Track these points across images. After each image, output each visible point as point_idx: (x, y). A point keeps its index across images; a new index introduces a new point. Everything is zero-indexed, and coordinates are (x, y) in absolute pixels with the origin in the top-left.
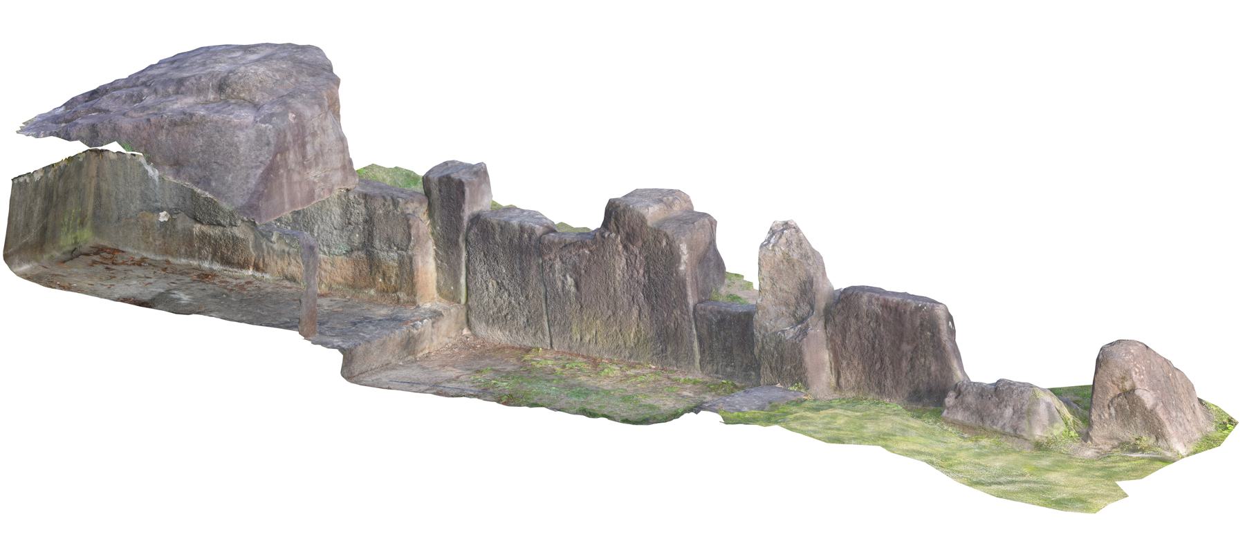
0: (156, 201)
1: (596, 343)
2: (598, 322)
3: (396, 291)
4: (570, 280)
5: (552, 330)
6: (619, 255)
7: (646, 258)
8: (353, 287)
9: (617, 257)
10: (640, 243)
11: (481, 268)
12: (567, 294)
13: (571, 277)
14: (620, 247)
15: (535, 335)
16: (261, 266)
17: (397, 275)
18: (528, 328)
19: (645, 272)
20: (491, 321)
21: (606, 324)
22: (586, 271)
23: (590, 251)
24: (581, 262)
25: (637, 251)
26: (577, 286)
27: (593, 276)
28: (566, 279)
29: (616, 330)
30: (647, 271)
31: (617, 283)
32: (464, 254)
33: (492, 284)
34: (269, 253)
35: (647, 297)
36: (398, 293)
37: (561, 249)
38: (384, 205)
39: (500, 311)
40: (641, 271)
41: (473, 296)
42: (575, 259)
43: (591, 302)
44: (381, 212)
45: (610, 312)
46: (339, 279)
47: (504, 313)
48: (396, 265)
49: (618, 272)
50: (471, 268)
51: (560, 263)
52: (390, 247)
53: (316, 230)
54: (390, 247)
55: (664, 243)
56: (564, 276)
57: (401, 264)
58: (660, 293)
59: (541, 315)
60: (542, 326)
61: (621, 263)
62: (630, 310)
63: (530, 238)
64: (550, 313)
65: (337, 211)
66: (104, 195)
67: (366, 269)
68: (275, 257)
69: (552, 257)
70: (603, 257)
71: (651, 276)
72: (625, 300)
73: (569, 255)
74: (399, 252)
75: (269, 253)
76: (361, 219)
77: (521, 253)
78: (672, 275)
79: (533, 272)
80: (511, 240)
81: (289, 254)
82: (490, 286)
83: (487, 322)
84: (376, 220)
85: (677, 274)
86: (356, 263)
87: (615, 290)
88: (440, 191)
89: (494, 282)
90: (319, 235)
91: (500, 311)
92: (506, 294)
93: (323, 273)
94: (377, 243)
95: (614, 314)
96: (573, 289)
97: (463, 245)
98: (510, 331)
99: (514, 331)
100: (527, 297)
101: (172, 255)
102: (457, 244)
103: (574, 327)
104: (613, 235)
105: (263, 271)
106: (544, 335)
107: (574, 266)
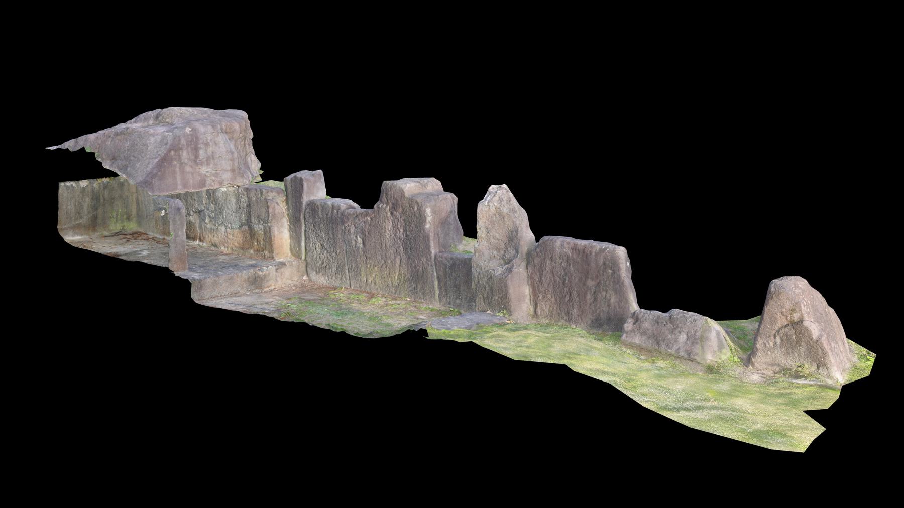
0: (159, 204)
1: (375, 283)
2: (376, 268)
3: (263, 251)
4: (360, 240)
5: (350, 275)
6: (388, 220)
7: (404, 220)
8: (242, 249)
9: (387, 222)
10: (401, 210)
11: (312, 235)
12: (358, 249)
13: (360, 237)
14: (389, 214)
15: (341, 278)
16: (202, 238)
17: (263, 240)
18: (337, 275)
19: (404, 231)
20: (318, 270)
21: (381, 270)
22: (368, 233)
23: (371, 218)
24: (365, 227)
25: (398, 216)
26: (364, 244)
27: (372, 236)
28: (357, 239)
29: (386, 274)
30: (405, 231)
31: (387, 240)
32: (303, 227)
33: (318, 245)
34: (205, 230)
35: (405, 249)
36: (264, 252)
37: (354, 218)
38: (256, 194)
39: (322, 263)
40: (402, 231)
41: (309, 254)
42: (362, 224)
43: (372, 254)
44: (254, 199)
45: (383, 261)
46: (236, 244)
47: (325, 264)
48: (262, 233)
49: (388, 232)
50: (307, 236)
51: (354, 228)
52: (259, 222)
53: (224, 214)
54: (259, 222)
55: (416, 209)
56: (356, 237)
57: (265, 232)
58: (413, 246)
59: (344, 265)
60: (345, 273)
61: (389, 226)
62: (395, 259)
63: (338, 212)
64: (349, 263)
65: (233, 200)
66: (140, 204)
67: (249, 238)
68: (208, 233)
69: (349, 225)
70: (378, 222)
71: (408, 233)
72: (392, 252)
73: (358, 222)
74: (264, 224)
75: (205, 230)
76: (245, 205)
77: (333, 223)
78: (421, 232)
79: (339, 236)
80: (327, 215)
81: (214, 230)
82: (317, 247)
83: (316, 271)
84: (252, 205)
85: (424, 231)
86: (244, 233)
87: (385, 245)
88: (292, 186)
89: (319, 244)
90: (226, 217)
91: (322, 263)
92: (326, 252)
93: (229, 241)
94: (253, 220)
95: (385, 262)
96: (361, 246)
97: (303, 221)
98: (328, 277)
99: (330, 277)
100: (336, 253)
101: (167, 236)
102: (299, 220)
103: (362, 273)
104: (385, 205)
105: (203, 242)
106: (346, 279)
107: (362, 230)
